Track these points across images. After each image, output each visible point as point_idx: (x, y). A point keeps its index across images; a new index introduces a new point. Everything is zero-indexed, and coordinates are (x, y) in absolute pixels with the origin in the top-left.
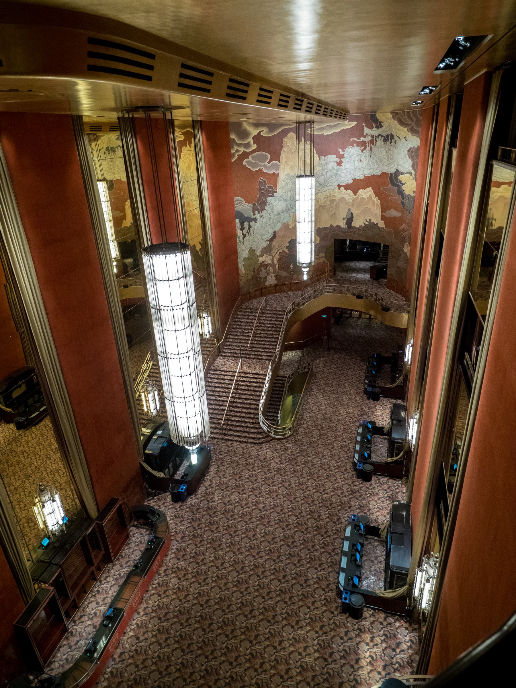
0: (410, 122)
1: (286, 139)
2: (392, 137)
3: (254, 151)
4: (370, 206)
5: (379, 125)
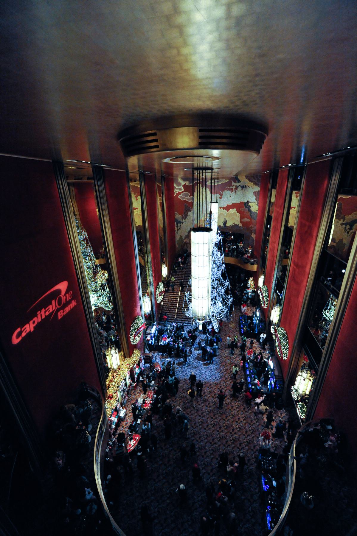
0: (254, 180)
2: (246, 186)
3: (183, 192)
4: (235, 217)
5: (239, 181)
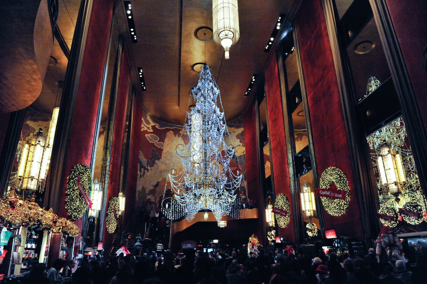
1: (168, 133)
